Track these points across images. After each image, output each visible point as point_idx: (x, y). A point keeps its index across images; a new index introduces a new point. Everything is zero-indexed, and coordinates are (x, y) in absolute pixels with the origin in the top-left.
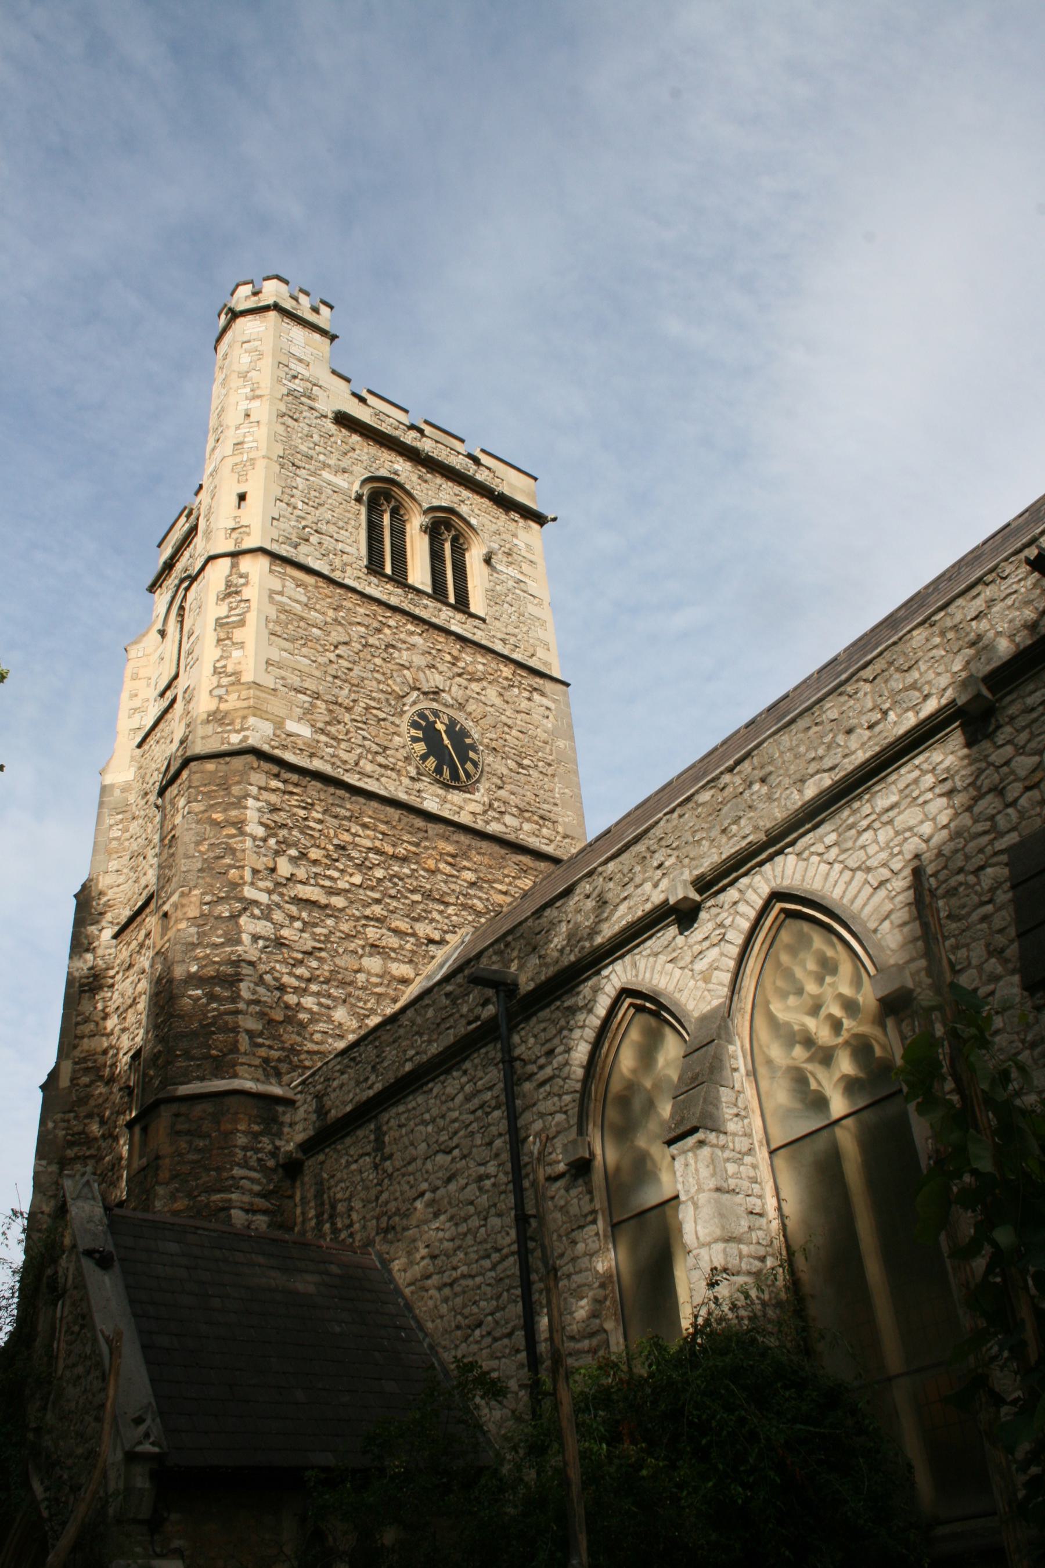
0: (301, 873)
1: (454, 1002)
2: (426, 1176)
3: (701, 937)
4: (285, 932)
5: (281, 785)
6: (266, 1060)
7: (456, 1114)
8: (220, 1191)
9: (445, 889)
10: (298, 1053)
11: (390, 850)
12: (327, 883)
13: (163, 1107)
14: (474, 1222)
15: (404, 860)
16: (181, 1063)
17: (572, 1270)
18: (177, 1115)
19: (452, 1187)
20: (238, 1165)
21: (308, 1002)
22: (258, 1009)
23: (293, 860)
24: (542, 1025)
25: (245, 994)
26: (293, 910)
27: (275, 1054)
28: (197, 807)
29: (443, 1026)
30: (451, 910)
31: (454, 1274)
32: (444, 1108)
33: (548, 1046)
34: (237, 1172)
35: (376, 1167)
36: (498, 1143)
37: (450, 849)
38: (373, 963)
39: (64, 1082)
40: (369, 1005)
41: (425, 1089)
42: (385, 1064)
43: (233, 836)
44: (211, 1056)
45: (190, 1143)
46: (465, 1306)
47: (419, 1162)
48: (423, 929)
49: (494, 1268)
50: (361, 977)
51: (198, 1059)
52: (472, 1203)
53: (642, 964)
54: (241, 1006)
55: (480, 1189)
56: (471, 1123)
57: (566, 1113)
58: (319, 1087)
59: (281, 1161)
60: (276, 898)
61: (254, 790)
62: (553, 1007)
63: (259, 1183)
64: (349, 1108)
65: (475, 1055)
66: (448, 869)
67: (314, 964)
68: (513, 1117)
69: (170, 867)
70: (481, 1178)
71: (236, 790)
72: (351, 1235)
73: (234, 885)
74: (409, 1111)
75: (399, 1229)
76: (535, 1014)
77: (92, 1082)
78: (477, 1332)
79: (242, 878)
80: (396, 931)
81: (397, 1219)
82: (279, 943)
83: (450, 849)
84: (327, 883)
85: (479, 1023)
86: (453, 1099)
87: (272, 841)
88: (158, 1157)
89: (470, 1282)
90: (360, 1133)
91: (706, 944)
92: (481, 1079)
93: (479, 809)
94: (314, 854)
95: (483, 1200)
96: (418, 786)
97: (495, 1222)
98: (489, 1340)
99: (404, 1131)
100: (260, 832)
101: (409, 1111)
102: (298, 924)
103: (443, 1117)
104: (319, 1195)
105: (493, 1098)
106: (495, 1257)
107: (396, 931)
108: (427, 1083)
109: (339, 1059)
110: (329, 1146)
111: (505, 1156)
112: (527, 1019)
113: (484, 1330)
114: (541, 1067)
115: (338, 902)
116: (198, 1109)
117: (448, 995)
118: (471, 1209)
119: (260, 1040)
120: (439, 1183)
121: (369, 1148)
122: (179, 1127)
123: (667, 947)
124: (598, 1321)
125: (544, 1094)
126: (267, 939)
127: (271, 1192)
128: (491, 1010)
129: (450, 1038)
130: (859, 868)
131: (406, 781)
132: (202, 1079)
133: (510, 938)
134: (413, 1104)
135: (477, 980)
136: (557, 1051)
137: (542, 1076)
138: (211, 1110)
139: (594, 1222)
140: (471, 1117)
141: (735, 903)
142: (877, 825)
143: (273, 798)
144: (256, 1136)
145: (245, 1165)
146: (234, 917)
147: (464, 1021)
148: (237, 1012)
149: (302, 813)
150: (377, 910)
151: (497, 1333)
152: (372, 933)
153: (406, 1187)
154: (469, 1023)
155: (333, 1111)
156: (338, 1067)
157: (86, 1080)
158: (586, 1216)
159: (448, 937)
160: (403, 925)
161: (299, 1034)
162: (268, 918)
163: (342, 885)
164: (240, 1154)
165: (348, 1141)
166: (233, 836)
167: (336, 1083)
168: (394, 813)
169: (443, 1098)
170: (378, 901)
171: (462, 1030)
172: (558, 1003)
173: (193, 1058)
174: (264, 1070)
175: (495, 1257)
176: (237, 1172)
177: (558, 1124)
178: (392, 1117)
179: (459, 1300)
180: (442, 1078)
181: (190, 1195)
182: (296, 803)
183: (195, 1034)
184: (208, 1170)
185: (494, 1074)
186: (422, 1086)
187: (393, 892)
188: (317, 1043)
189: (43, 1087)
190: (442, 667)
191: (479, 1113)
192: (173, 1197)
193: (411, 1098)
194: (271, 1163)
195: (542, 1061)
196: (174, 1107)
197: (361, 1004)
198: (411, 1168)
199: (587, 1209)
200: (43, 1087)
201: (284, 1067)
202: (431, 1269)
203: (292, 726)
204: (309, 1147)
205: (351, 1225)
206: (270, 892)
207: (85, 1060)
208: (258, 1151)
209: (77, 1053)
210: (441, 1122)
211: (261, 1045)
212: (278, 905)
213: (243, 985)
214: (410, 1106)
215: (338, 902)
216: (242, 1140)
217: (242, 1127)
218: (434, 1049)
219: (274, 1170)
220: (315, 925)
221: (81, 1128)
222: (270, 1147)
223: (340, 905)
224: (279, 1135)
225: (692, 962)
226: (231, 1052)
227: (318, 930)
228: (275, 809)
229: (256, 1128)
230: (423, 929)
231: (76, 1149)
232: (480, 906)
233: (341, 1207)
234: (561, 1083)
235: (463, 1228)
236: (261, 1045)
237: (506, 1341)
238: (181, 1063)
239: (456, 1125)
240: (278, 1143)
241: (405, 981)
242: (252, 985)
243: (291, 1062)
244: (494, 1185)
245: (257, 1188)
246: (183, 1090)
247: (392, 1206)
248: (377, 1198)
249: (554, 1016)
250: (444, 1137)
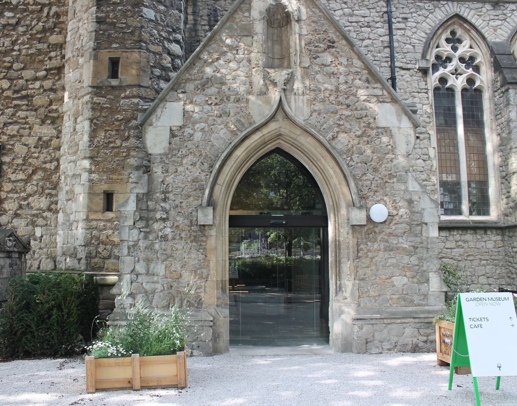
3: (495, 14)
24: (402, 6)
53: (463, 9)
56: (349, 26)
86: (335, 11)
91: (497, 18)
92: (358, 10)
123: (477, 9)
124: (424, 129)
125: (401, 34)
136: (409, 20)
140: (349, 24)
141: (513, 10)
177: (407, 49)
225: (489, 21)
249: (409, 5)
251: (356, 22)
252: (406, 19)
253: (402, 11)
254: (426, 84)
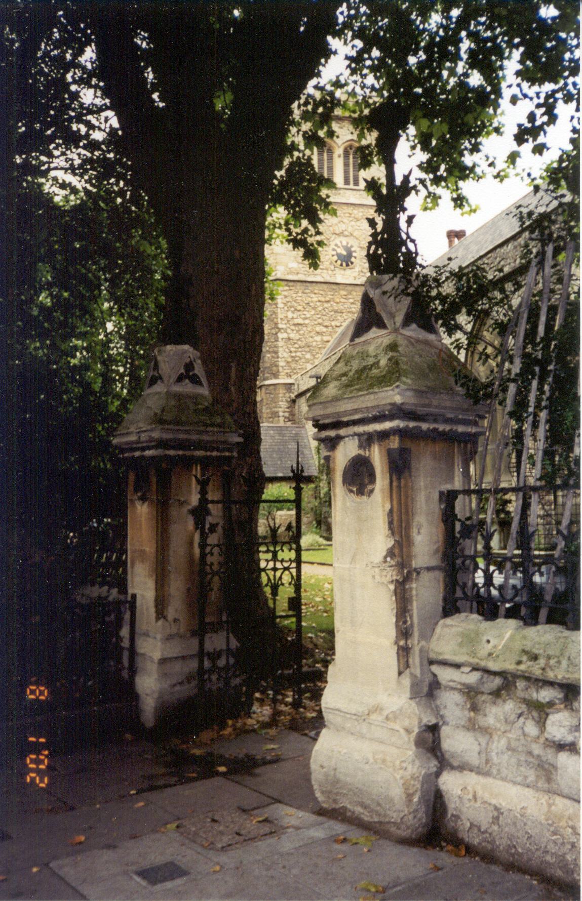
0: (295, 316)
15: (328, 302)
21: (299, 354)
23: (293, 312)
26: (293, 327)
37: (345, 293)
38: (318, 338)
48: (333, 323)
80: (326, 327)
82: (289, 339)
83: (345, 293)
94: (299, 308)
107: (326, 327)
115: (307, 322)
116: (271, 387)
131: (330, 272)
143: (286, 293)
146: (276, 334)
150: (320, 321)
152: (318, 329)
163: (308, 316)
168: (325, 286)
190: (345, 221)
203: (290, 265)
215: (307, 322)
228: (286, 297)
230: (333, 323)
241: (328, 341)
246: (267, 382)
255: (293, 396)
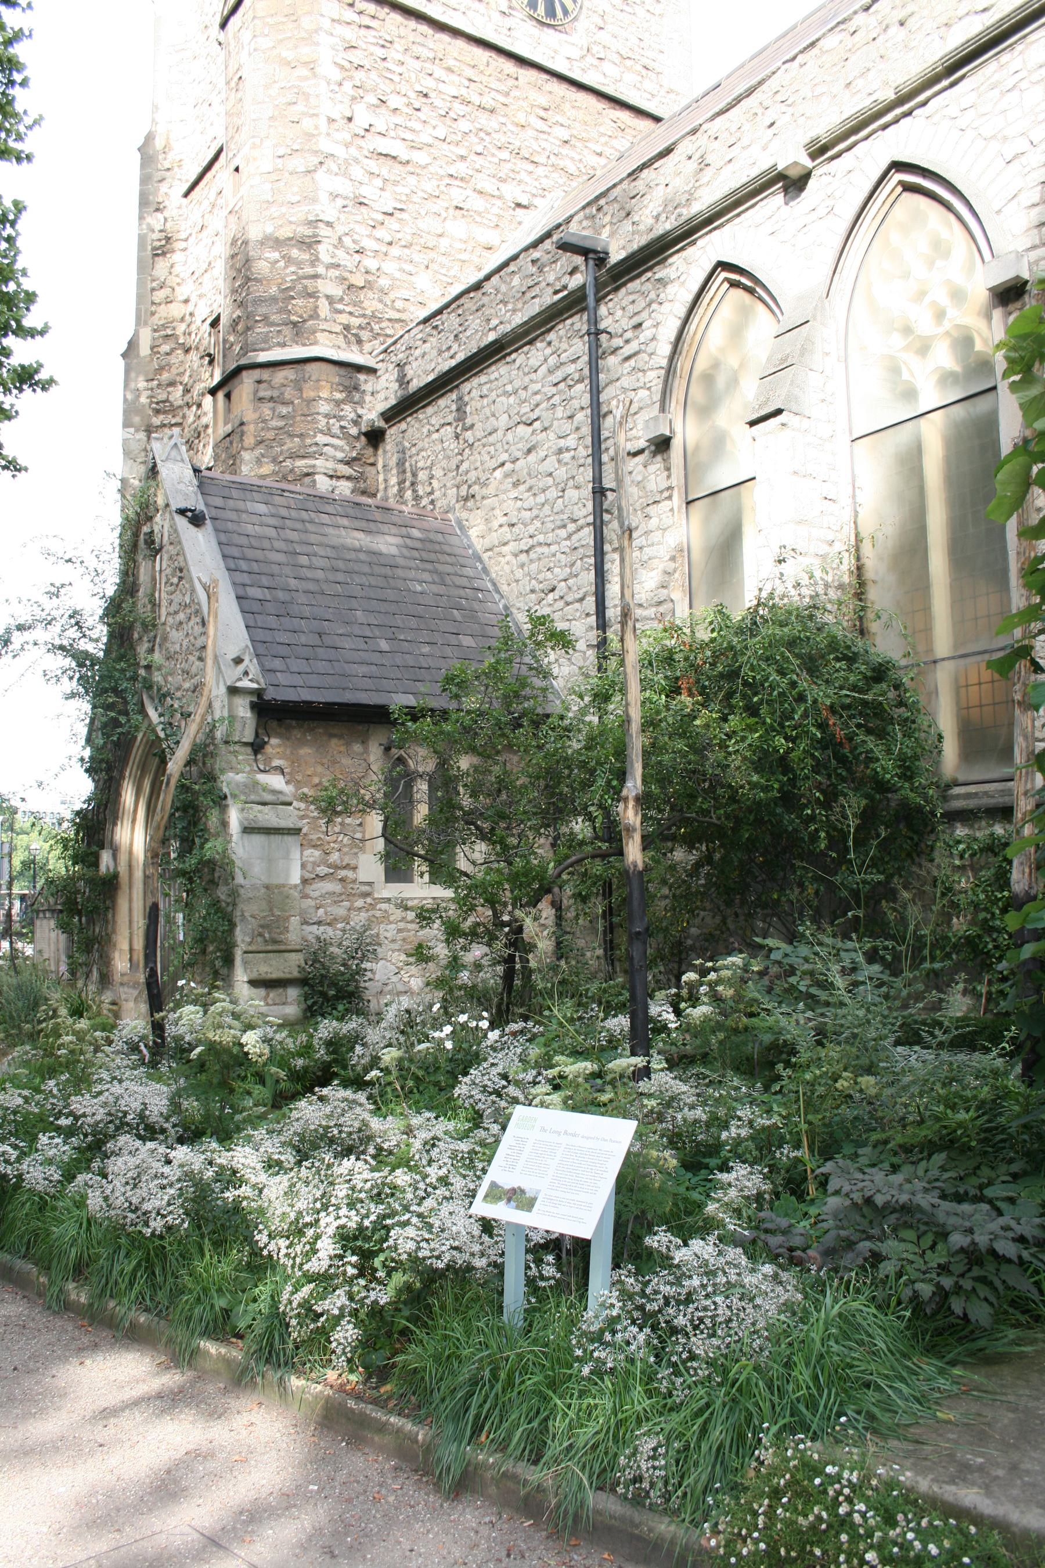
1: (541, 270)
2: (506, 447)
4: (364, 191)
5: (355, 17)
6: (347, 328)
7: (537, 387)
8: (304, 457)
9: (536, 147)
10: (380, 320)
11: (476, 99)
12: (408, 136)
13: (244, 373)
14: (552, 493)
16: (261, 329)
17: (644, 543)
18: (259, 382)
19: (532, 458)
20: (322, 432)
22: (337, 273)
24: (631, 298)
25: (325, 257)
26: (373, 165)
27: (355, 322)
28: (264, 43)
29: (529, 295)
30: (540, 171)
31: (531, 542)
32: (527, 379)
33: (636, 320)
34: (321, 439)
35: (457, 437)
36: (580, 416)
38: (457, 227)
39: (144, 350)
40: (452, 273)
41: (508, 359)
42: (468, 333)
43: (306, 78)
44: (292, 323)
45: (273, 410)
46: (540, 572)
47: (500, 433)
49: (569, 537)
50: (444, 242)
51: (278, 325)
52: (550, 475)
54: (321, 270)
55: (559, 461)
57: (649, 389)
58: (401, 356)
59: (364, 430)
60: (353, 151)
61: (326, 23)
62: (643, 278)
63: (343, 451)
64: (431, 378)
65: (560, 326)
66: (540, 125)
67: (396, 226)
68: (596, 391)
69: (239, 114)
70: (560, 451)
71: (306, 23)
72: (432, 502)
73: (309, 136)
74: (491, 382)
75: (478, 497)
76: (624, 284)
77: (173, 350)
78: (551, 596)
79: (317, 128)
81: (476, 487)
83: (543, 101)
84: (408, 136)
85: (566, 293)
87: (348, 86)
88: (242, 424)
89: (545, 550)
90: (442, 402)
93: (576, 54)
94: (394, 101)
95: (561, 473)
96: (509, 22)
97: (572, 494)
98: (561, 604)
99: (485, 401)
100: (336, 75)
101: (491, 382)
102: (378, 182)
103: (525, 388)
104: (401, 463)
105: (576, 371)
106: (571, 527)
108: (510, 354)
109: (421, 327)
110: (411, 415)
111: (586, 430)
112: (616, 289)
113: (556, 594)
114: (627, 342)
115: (420, 157)
117: (533, 262)
118: (550, 480)
119: (340, 307)
120: (519, 454)
121: (450, 418)
122: (261, 394)
124: (665, 591)
126: (346, 198)
127: (355, 459)
128: (578, 280)
129: (535, 308)
130: (993, 137)
132: (283, 345)
133: (602, 202)
134: (496, 375)
135: (565, 247)
137: (627, 350)
138: (293, 377)
139: (670, 498)
140: (554, 390)
142: (1024, 85)
144: (338, 403)
145: (328, 433)
147: (550, 290)
148: (316, 276)
149: (381, 52)
151: (569, 599)
152: (457, 195)
153: (487, 458)
154: (556, 292)
155: (415, 381)
156: (420, 336)
157: (165, 348)
158: (661, 492)
159: (537, 201)
160: (489, 186)
161: (381, 301)
162: (346, 174)
163: (424, 138)
164: (323, 422)
165: (430, 410)
166: (306, 78)
167: (417, 353)
168: (482, 55)
169: (526, 370)
170: (463, 158)
171: (549, 299)
172: (649, 274)
173: (273, 324)
174: (345, 337)
175: (571, 527)
176: (321, 439)
177: (642, 400)
178: (472, 387)
179: (534, 567)
180: (526, 349)
181: (274, 461)
182: (375, 41)
183: (274, 299)
184: (291, 436)
185: (580, 347)
186: (504, 357)
187: (480, 149)
188: (399, 311)
189: (124, 355)
191: (562, 385)
192: (259, 462)
193: (493, 368)
194: (354, 431)
195: (629, 335)
196: (256, 374)
197: (443, 271)
198: (492, 439)
199: (664, 485)
200: (124, 355)
201: (365, 335)
202: (509, 536)
204: (392, 415)
205: (431, 493)
206: (347, 146)
207: (164, 327)
208: (340, 418)
209: (156, 320)
210: (523, 394)
211: (340, 312)
212: (356, 161)
213: (321, 248)
214: (492, 377)
216: (324, 408)
217: (324, 394)
218: (518, 319)
219: (357, 438)
220: (396, 183)
221: (164, 397)
222: (353, 415)
223: (423, 162)
224: (361, 403)
226: (311, 317)
227: (399, 189)
229: (338, 396)
231: (161, 417)
232: (572, 169)
233: (422, 476)
234: (647, 358)
235: (541, 499)
236: (340, 312)
237: (577, 605)
238: (261, 329)
239: (538, 397)
240: (360, 411)
242: (331, 248)
243: (372, 330)
244: (573, 458)
245: (340, 455)
246: (263, 357)
247: (472, 476)
248: (458, 467)
249: (644, 288)
250: (525, 408)
251: (564, 380)
252: (639, 325)
253: (631, 309)
254: (669, 477)
255: (371, 413)
